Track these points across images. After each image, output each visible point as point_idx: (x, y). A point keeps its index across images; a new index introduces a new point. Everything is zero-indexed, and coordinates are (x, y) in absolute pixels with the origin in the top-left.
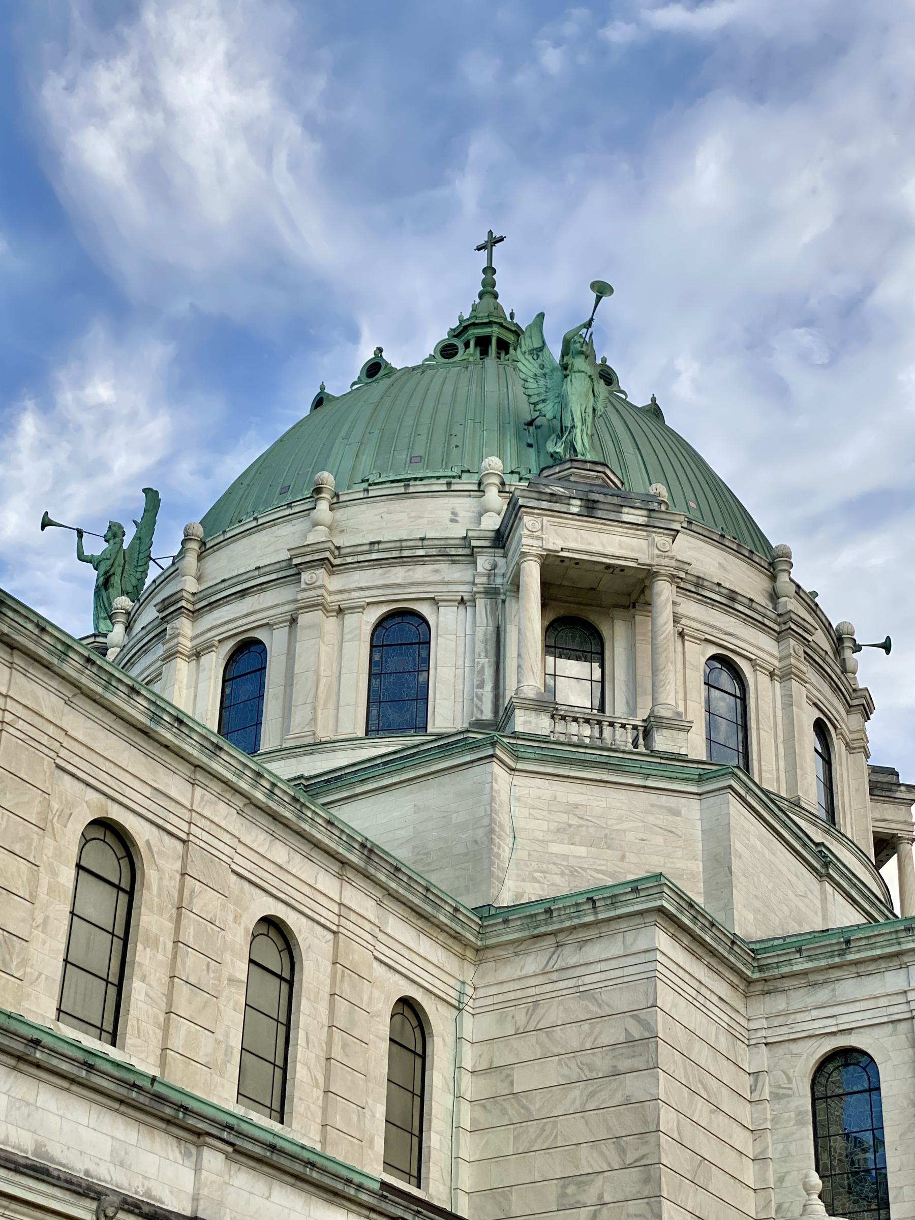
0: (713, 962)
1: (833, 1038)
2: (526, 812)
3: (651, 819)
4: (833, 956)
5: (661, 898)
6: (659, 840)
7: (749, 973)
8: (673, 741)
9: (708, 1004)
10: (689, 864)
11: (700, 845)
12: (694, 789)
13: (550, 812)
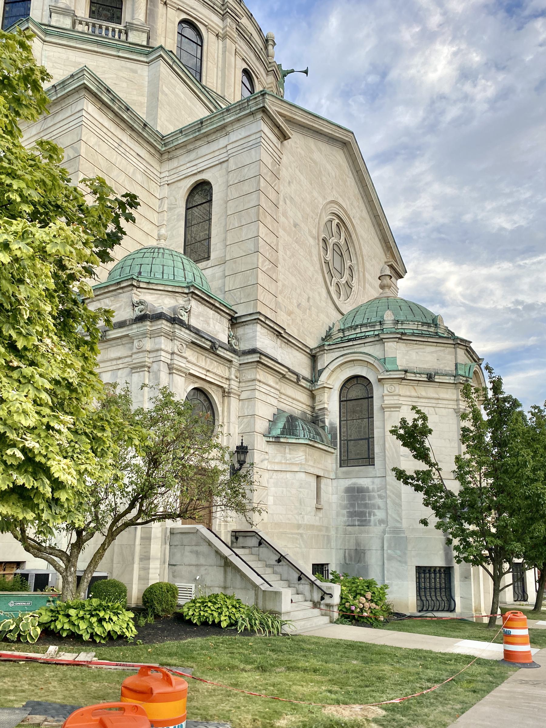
0: (133, 134)
1: (195, 176)
2: (51, 65)
3: (121, 74)
4: (195, 132)
5: (84, 79)
6: (124, 85)
7: (160, 148)
8: (139, 37)
9: (127, 154)
10: (140, 98)
11: (146, 89)
12: (145, 59)
13: (65, 65)
